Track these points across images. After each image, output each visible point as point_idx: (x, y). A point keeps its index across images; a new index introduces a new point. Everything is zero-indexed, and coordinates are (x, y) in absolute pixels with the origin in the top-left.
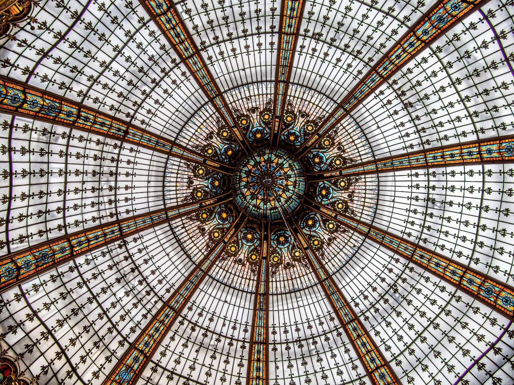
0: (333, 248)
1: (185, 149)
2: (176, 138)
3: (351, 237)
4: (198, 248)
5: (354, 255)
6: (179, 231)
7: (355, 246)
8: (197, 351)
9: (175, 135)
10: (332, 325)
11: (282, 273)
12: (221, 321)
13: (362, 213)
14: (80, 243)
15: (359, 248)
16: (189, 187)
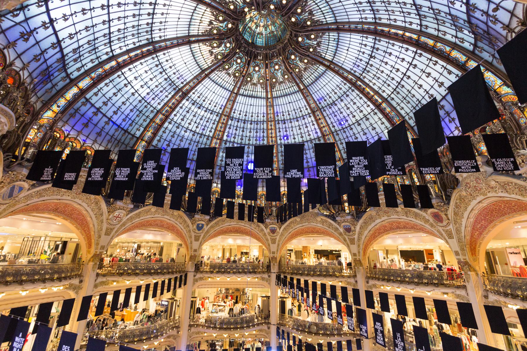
0: (323, 47)
1: (209, 68)
2: (201, 69)
3: (329, 36)
4: (260, 91)
5: (338, 44)
6: (246, 93)
7: (335, 39)
8: (292, 131)
9: (199, 69)
10: (346, 87)
11: (306, 75)
12: (293, 112)
13: (325, 18)
14: (219, 135)
15: (338, 39)
16: (230, 76)
